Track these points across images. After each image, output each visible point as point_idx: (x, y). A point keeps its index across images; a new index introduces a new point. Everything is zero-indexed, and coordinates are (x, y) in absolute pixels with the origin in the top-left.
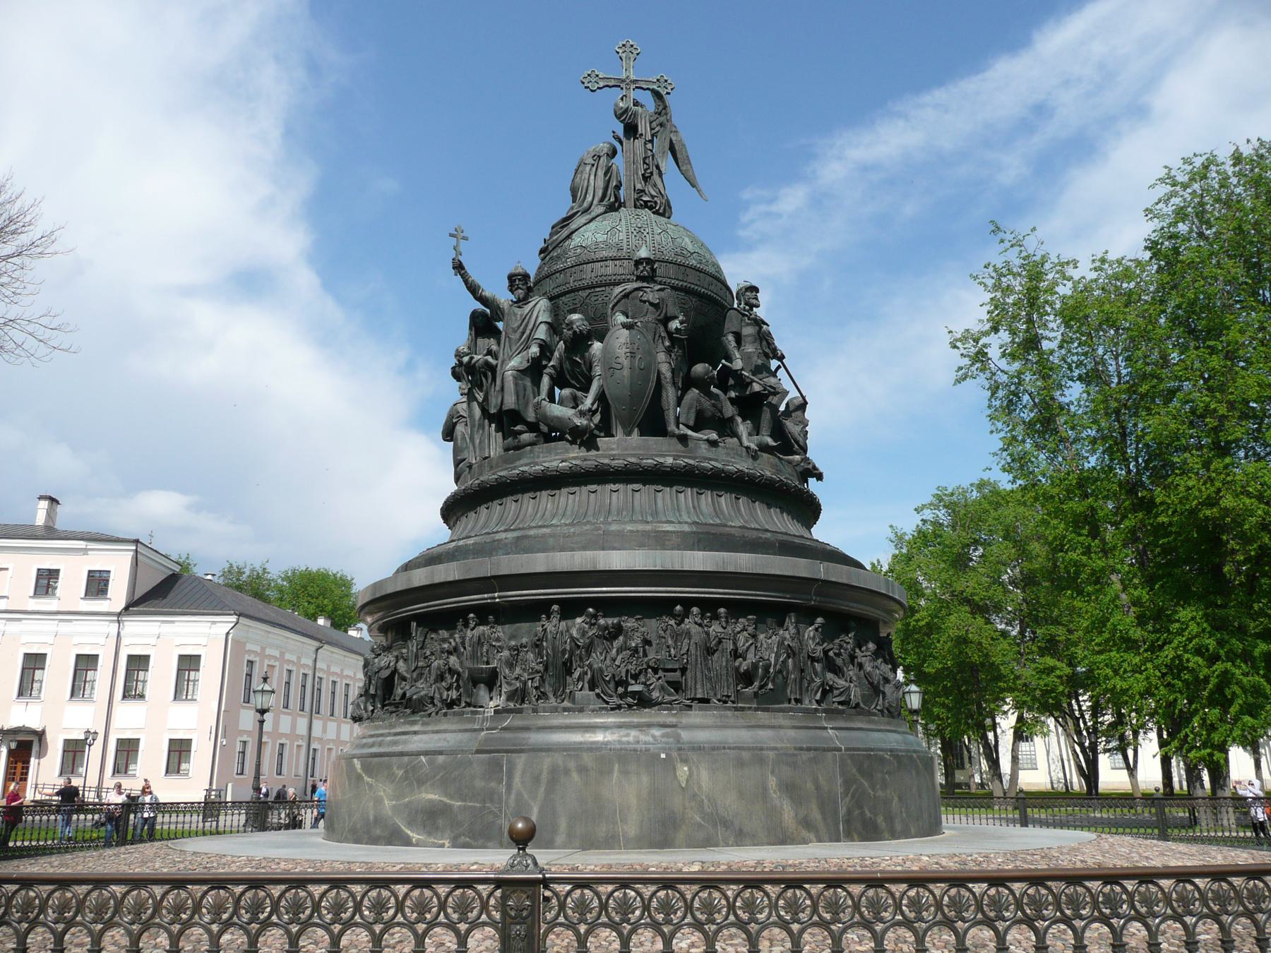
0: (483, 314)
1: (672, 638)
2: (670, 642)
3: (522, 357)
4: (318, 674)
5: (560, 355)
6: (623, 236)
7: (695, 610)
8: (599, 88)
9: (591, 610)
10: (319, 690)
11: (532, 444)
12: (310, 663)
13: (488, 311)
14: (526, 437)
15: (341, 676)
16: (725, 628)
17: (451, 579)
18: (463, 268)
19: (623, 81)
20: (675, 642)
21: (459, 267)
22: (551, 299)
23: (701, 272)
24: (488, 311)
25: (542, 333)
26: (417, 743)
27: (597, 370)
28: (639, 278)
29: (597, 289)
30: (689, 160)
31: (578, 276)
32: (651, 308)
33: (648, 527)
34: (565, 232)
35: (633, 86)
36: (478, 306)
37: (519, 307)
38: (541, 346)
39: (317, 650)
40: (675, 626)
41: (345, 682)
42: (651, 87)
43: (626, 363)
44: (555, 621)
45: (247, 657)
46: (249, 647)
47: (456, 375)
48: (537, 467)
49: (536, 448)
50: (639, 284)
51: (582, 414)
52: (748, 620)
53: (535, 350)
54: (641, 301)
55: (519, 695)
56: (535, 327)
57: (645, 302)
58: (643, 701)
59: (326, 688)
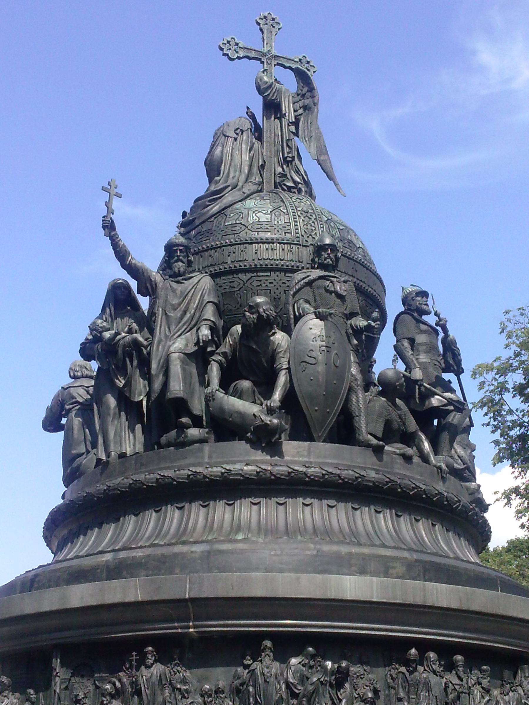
0: (126, 287)
1: (404, 688)
2: (402, 694)
3: (187, 340)
5: (234, 341)
7: (432, 655)
8: (239, 58)
9: (311, 649)
11: (203, 441)
13: (133, 284)
14: (194, 432)
16: (461, 679)
17: (131, 598)
18: (114, 229)
19: (264, 55)
20: (408, 693)
22: (213, 276)
23: (367, 269)
24: (133, 284)
28: (323, 266)
29: (261, 274)
30: (326, 150)
31: (233, 257)
32: (337, 300)
34: (215, 208)
35: (274, 62)
36: (124, 276)
37: (178, 282)
38: (211, 329)
40: (407, 674)
42: (294, 67)
43: (320, 357)
44: (267, 661)
48: (215, 469)
49: (206, 448)
50: (323, 273)
51: (270, 411)
52: (482, 671)
53: (205, 332)
54: (327, 291)
56: (201, 307)
57: (331, 292)
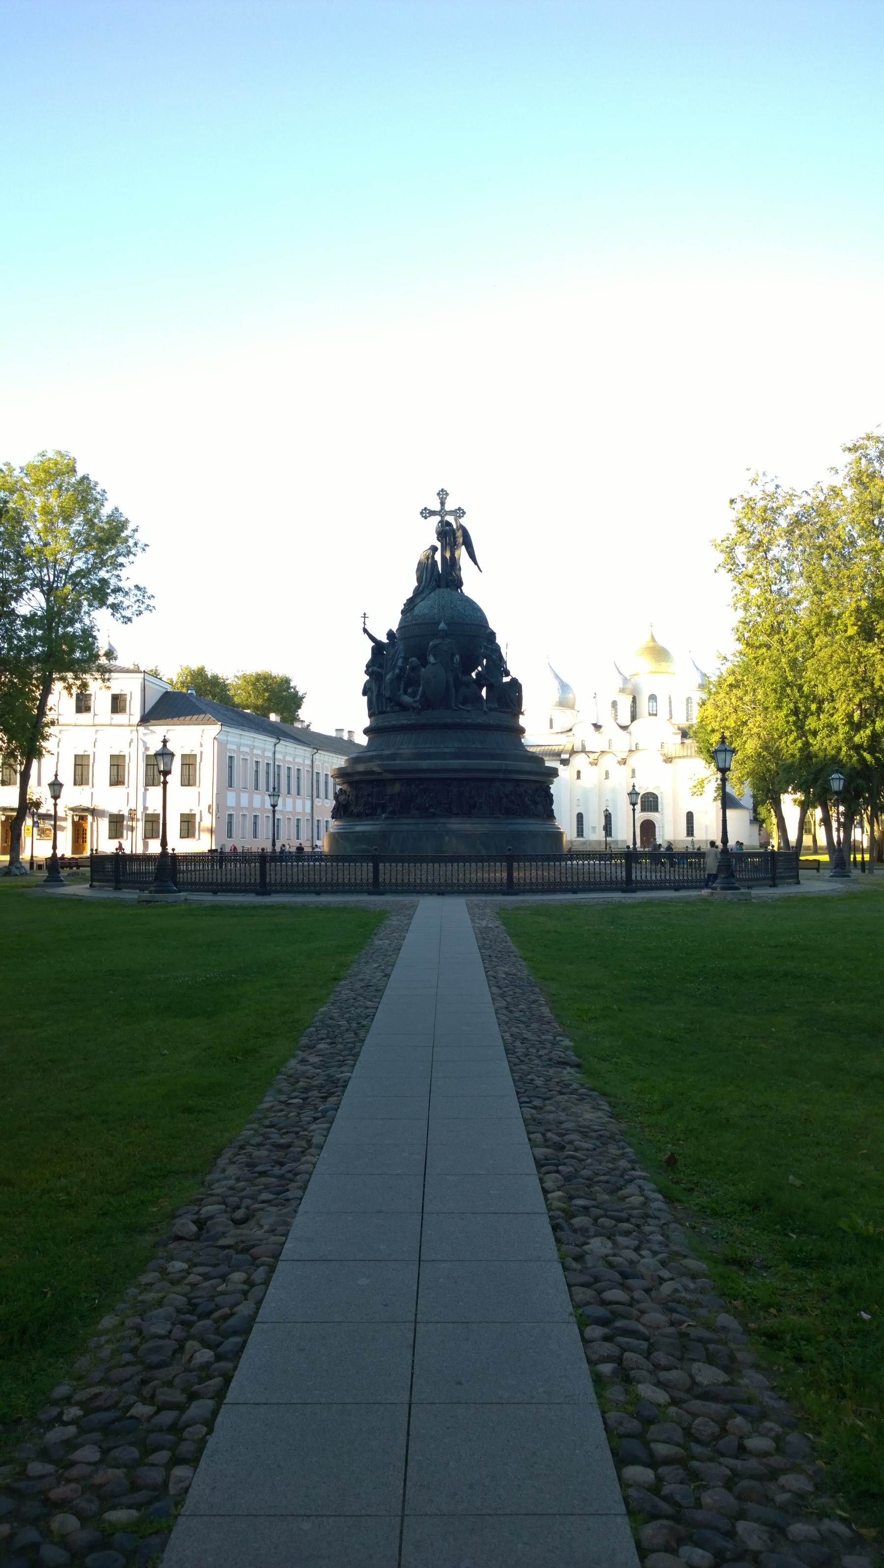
4: (277, 763)
6: (436, 611)
10: (279, 775)
12: (270, 755)
14: (397, 708)
15: (294, 763)
21: (365, 631)
25: (400, 663)
26: (359, 828)
27: (422, 682)
33: (439, 750)
39: (275, 745)
41: (297, 767)
45: (229, 754)
46: (229, 746)
47: (366, 672)
51: (416, 702)
53: (397, 671)
55: (393, 813)
58: (433, 815)
59: (284, 773)
